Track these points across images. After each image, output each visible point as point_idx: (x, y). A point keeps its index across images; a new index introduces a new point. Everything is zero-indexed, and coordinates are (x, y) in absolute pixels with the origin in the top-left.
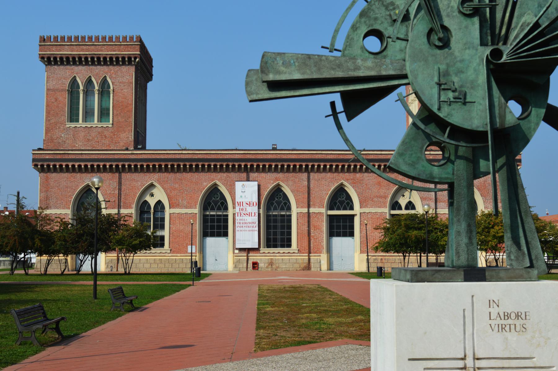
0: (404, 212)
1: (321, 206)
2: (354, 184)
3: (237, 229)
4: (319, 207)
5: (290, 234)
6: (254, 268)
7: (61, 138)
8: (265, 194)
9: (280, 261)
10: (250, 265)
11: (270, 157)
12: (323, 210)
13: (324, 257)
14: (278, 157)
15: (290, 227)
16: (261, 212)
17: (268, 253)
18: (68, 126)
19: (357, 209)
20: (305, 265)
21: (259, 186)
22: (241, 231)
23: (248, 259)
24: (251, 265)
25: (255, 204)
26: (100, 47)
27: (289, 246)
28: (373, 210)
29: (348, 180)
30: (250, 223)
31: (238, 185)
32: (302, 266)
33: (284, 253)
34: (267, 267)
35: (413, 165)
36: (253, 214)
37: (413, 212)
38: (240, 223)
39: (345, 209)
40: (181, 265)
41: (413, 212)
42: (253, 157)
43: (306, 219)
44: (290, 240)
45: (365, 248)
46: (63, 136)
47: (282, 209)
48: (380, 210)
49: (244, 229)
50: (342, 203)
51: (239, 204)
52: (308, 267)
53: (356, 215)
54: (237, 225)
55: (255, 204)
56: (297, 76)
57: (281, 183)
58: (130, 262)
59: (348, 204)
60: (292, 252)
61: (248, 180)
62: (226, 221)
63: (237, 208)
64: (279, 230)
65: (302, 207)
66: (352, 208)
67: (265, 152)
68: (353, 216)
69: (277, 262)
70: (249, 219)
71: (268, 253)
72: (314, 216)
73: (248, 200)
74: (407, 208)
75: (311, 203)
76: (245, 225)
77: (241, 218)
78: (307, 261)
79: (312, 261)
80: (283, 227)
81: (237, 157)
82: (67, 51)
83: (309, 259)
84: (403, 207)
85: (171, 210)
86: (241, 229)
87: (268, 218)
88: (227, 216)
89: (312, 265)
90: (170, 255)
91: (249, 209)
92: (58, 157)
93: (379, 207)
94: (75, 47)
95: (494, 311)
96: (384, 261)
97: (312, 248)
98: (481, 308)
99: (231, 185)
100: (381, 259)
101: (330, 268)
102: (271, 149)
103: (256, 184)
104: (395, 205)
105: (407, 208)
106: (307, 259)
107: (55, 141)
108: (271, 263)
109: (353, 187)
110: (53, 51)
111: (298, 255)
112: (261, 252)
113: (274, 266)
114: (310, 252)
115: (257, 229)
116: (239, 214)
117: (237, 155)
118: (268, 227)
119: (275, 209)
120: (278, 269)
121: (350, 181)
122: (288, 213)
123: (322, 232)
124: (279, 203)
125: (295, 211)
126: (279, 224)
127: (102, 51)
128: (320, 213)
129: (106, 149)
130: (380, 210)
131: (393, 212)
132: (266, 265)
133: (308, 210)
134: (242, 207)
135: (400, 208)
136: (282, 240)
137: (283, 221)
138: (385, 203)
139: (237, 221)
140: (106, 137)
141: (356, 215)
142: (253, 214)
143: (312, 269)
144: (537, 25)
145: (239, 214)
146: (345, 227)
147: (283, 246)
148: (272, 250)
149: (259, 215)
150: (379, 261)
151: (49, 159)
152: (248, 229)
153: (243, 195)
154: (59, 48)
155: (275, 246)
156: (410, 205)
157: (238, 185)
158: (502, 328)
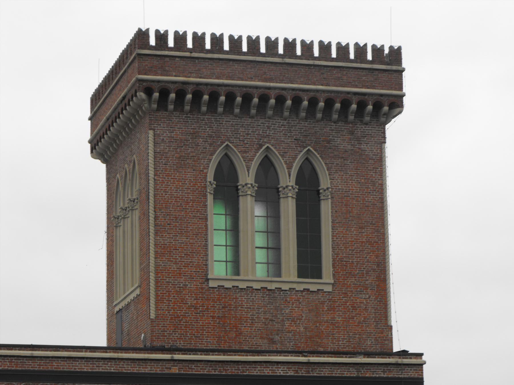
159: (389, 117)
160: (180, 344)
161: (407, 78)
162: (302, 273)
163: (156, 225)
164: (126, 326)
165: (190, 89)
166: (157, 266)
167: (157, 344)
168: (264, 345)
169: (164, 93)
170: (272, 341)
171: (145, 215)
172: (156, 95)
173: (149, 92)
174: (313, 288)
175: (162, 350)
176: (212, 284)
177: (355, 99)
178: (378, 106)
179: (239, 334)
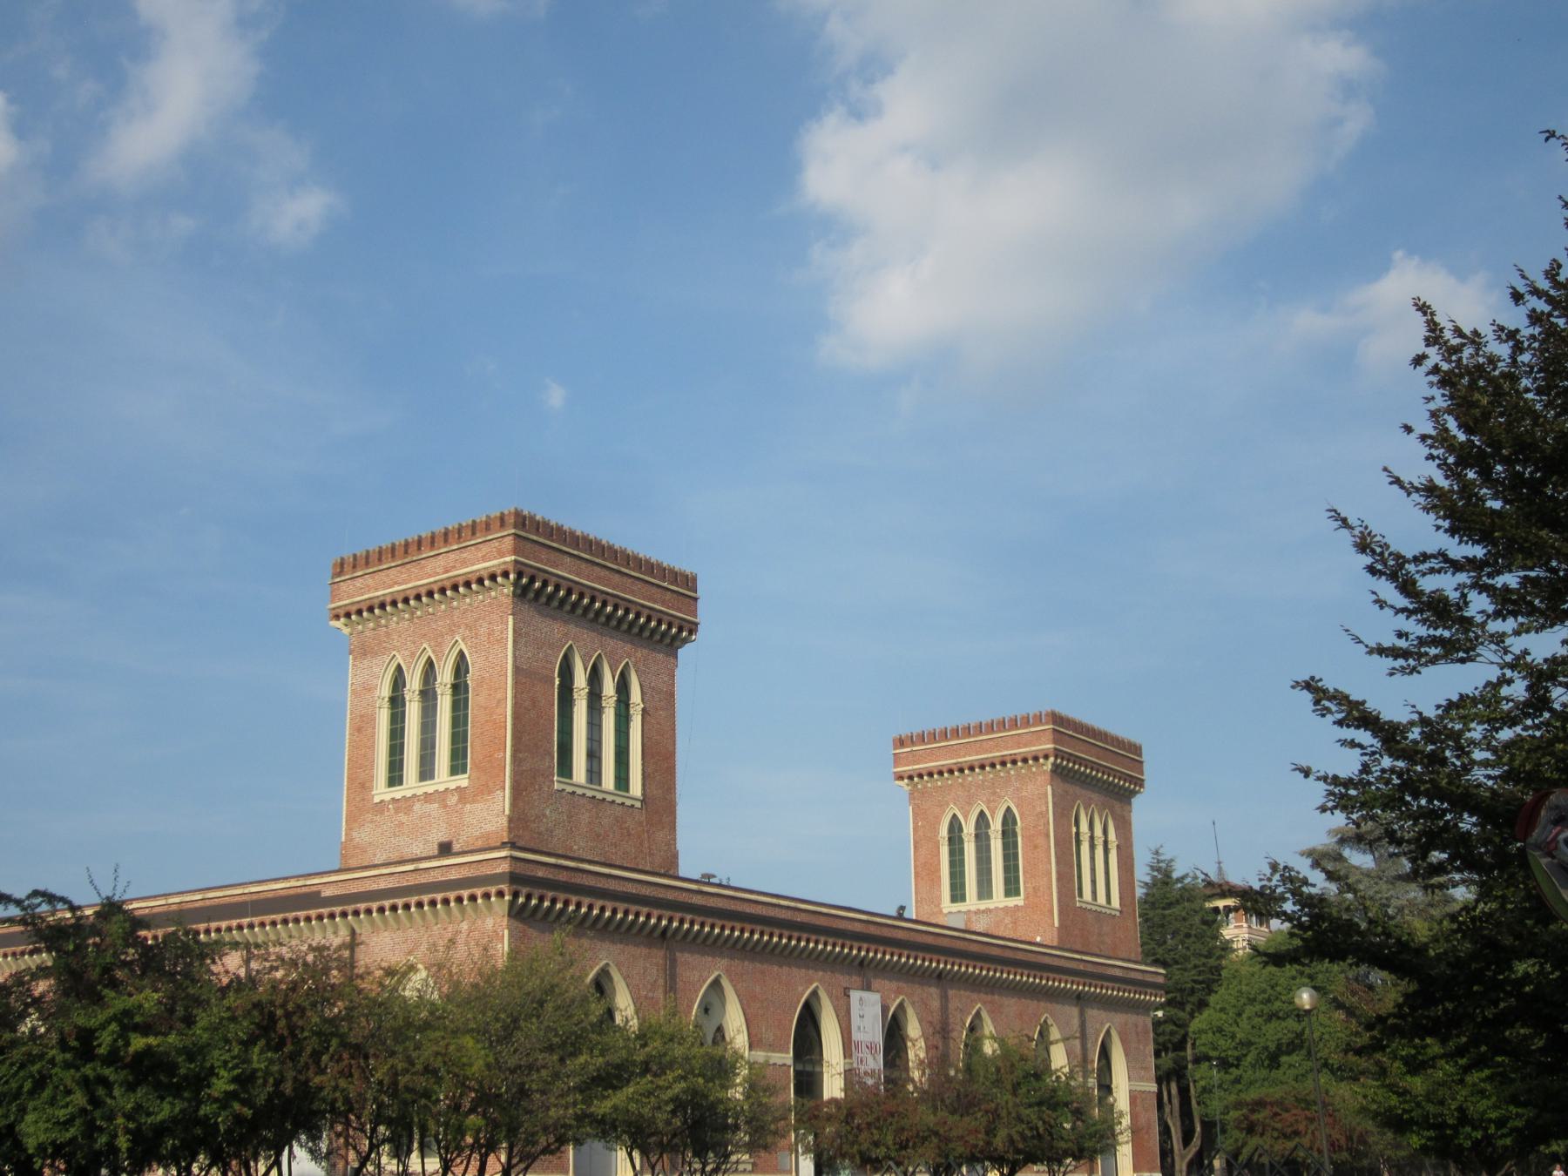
7: (544, 820)
18: (556, 786)
26: (630, 581)
31: (855, 995)
46: (548, 812)
82: (569, 572)
85: (753, 1053)
92: (563, 877)
94: (584, 565)
102: (894, 913)
107: (533, 826)
110: (540, 561)
117: (856, 924)
127: (632, 593)
129: (628, 865)
140: (629, 835)
151: (542, 878)
154: (553, 556)
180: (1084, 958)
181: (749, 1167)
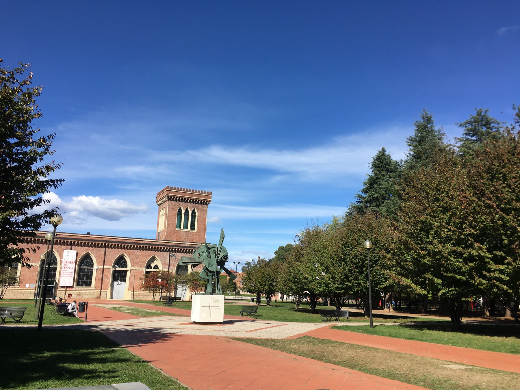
0: (153, 270)
1: (111, 265)
2: (129, 255)
3: (61, 275)
4: (109, 266)
5: (91, 279)
6: (69, 297)
8: (80, 257)
9: (84, 294)
10: (67, 295)
11: (85, 238)
12: (111, 267)
13: (109, 292)
14: (90, 238)
15: (91, 276)
16: (76, 267)
17: (78, 289)
19: (129, 267)
20: (98, 296)
21: (77, 253)
22: (64, 276)
23: (66, 292)
24: (67, 295)
25: (73, 262)
27: (90, 285)
28: (137, 268)
29: (126, 252)
30: (69, 272)
32: (96, 296)
33: (87, 289)
34: (76, 297)
35: (203, 276)
36: (72, 268)
37: (158, 270)
38: (64, 272)
39: (123, 267)
40: (25, 295)
41: (158, 270)
42: (76, 237)
43: (102, 272)
44: (91, 282)
45: (132, 287)
47: (89, 266)
48: (141, 269)
49: (66, 275)
50: (121, 264)
51: (66, 262)
52: (100, 297)
53: (128, 271)
54: (62, 273)
55: (73, 262)
56: (187, 261)
57: (90, 252)
58: (4, 292)
59: (125, 265)
60: (91, 289)
61: (71, 249)
62: (55, 271)
63: (63, 265)
64: (85, 277)
65: (100, 265)
66: (126, 267)
67: (83, 235)
68: (126, 271)
69: (82, 294)
70: (69, 270)
71: (78, 289)
72: (106, 270)
73: (70, 261)
74: (154, 268)
75: (105, 263)
76: (67, 273)
77: (65, 269)
78: (99, 294)
79: (102, 294)
80: (88, 275)
81: (66, 237)
83: (101, 293)
84: (153, 268)
86: (64, 275)
87: (80, 270)
88: (56, 268)
89: (102, 296)
90: (19, 289)
91: (70, 265)
93: (141, 267)
95: (214, 299)
96: (140, 294)
97: (103, 287)
98: (213, 299)
99: (61, 252)
100: (139, 294)
101: (112, 297)
103: (75, 252)
104: (148, 266)
105: (154, 268)
106: (100, 293)
108: (79, 295)
109: (128, 256)
111: (95, 290)
112: (74, 288)
113: (80, 296)
114: (101, 289)
115: (73, 276)
116: (64, 268)
118: (79, 275)
119: (85, 265)
120: (83, 298)
121: (127, 253)
122: (91, 268)
123: (109, 279)
124: (87, 262)
125: (95, 267)
126: (86, 274)
128: (109, 269)
130: (141, 269)
131: (147, 270)
132: (76, 295)
133: (103, 267)
134: (66, 264)
135: (151, 268)
136: (87, 282)
137: (88, 272)
138: (144, 265)
139: (62, 271)
141: (128, 271)
142: (72, 268)
143: (102, 298)
144: (224, 255)
145: (64, 268)
146: (121, 277)
147: (86, 285)
148: (80, 287)
149: (75, 268)
150: (138, 294)
152: (68, 276)
153: (67, 257)
155: (82, 285)
156: (156, 267)
157: (66, 252)
158: (215, 302)
159: (209, 203)
160: (170, 240)
161: (212, 197)
162: (191, 229)
163: (168, 219)
164: (160, 235)
165: (176, 197)
166: (167, 226)
167: (166, 240)
168: (184, 241)
169: (171, 197)
170: (186, 240)
171: (166, 217)
172: (169, 197)
173: (168, 197)
174: (193, 231)
175: (167, 241)
176: (176, 230)
177: (203, 200)
178: (207, 202)
179: (180, 238)
180: (169, 242)
181: (18, 287)
